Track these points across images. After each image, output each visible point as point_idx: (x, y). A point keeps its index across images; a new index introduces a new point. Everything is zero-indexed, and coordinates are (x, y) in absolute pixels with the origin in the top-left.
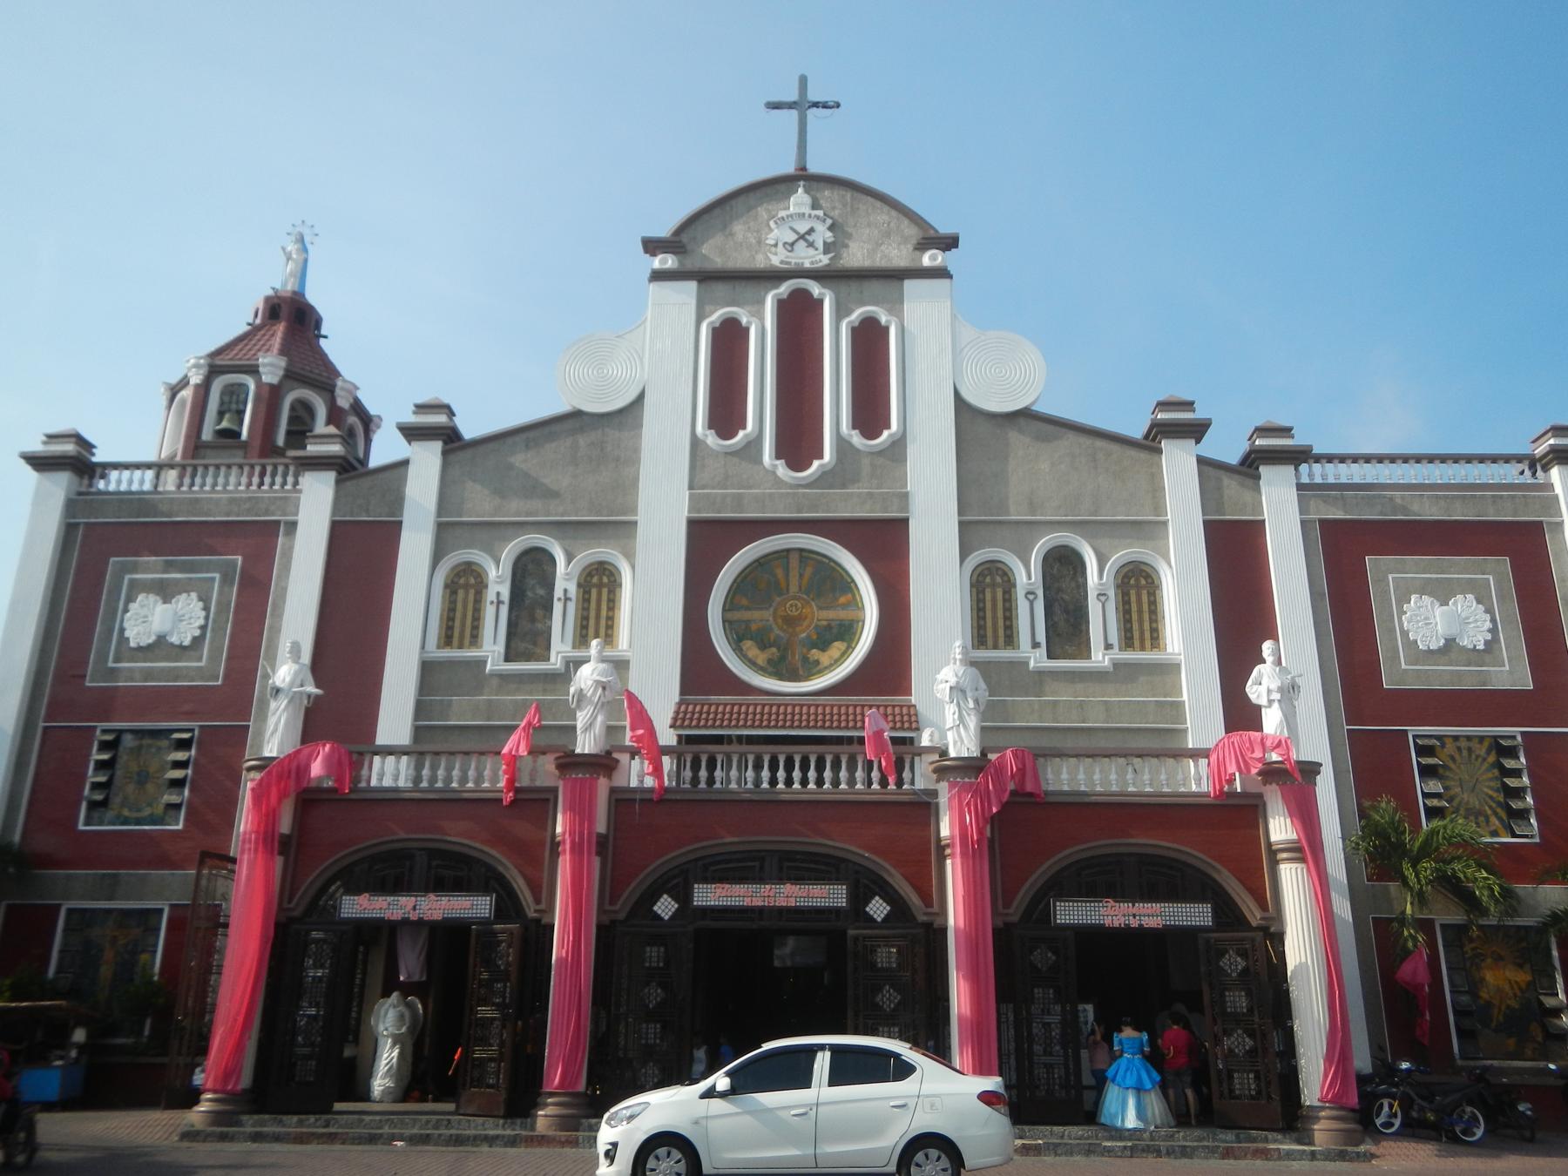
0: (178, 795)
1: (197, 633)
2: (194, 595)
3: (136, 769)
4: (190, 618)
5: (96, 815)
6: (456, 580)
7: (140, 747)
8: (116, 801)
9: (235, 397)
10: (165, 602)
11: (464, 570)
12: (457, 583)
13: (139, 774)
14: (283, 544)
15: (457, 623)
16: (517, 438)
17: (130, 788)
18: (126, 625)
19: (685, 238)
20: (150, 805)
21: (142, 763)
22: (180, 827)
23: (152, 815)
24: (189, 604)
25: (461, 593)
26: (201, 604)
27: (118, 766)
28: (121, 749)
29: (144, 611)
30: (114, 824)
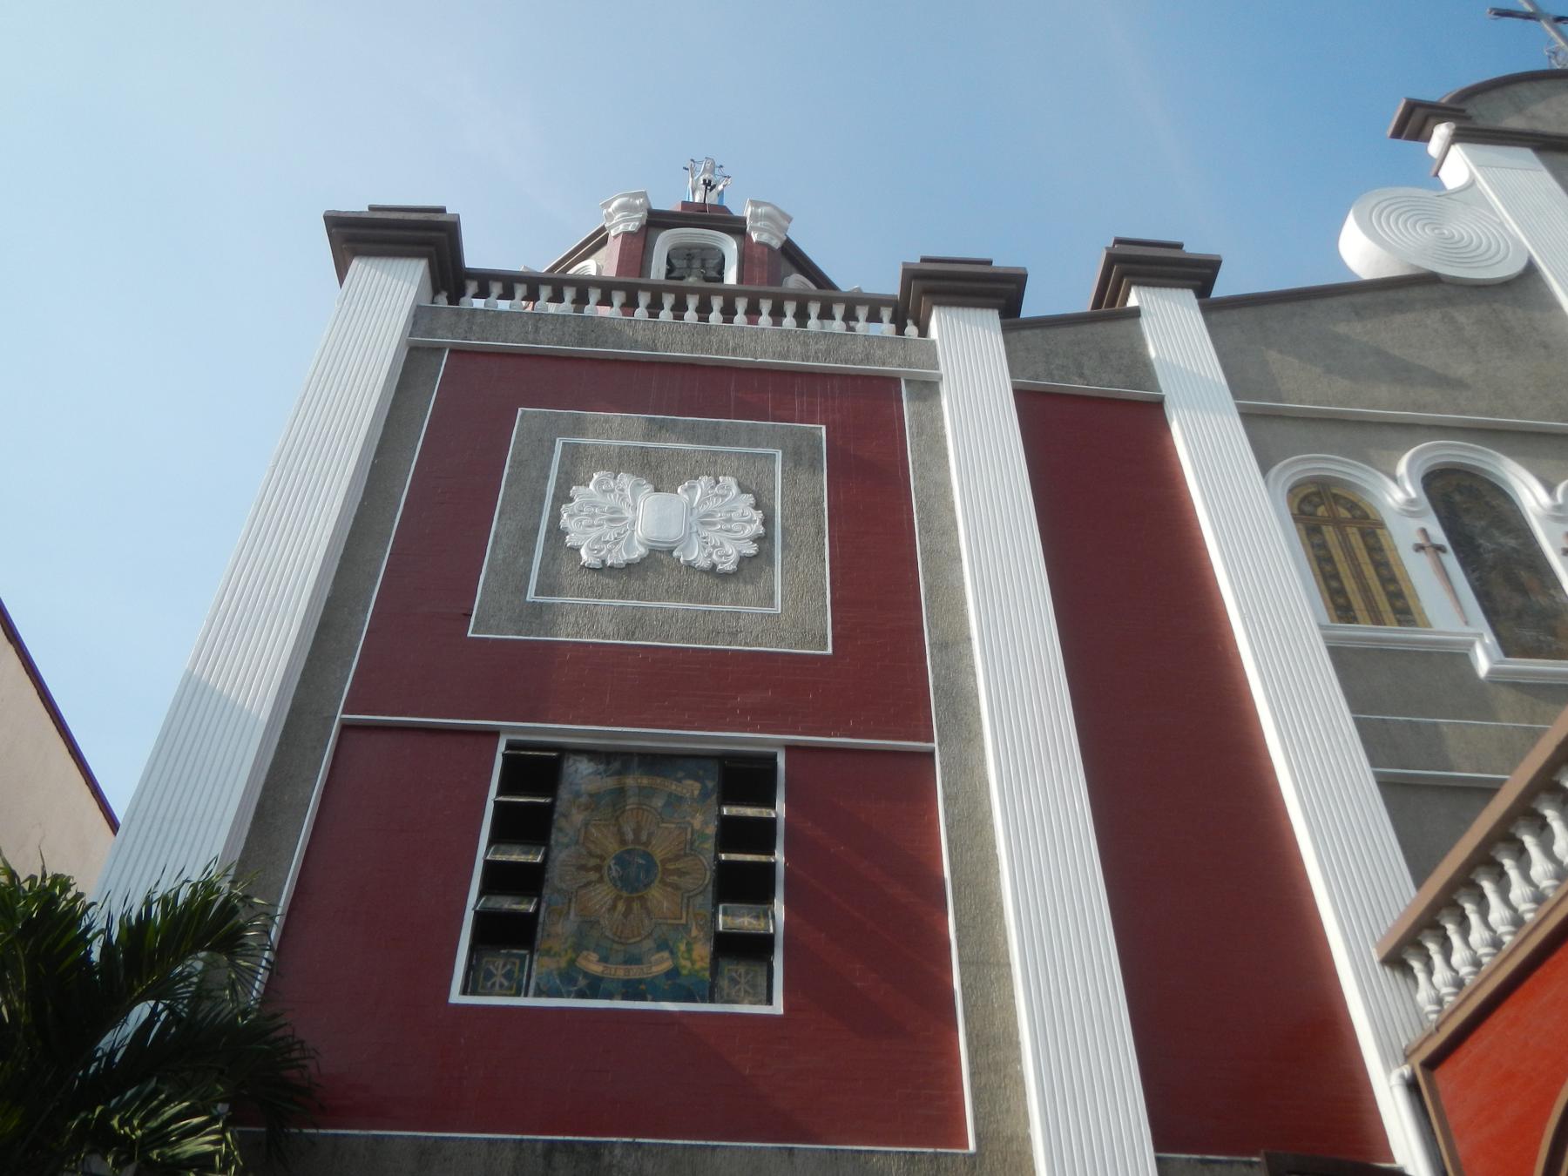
0: (757, 917)
1: (751, 549)
2: (729, 482)
3: (613, 847)
4: (729, 520)
5: (498, 964)
6: (1307, 508)
7: (621, 792)
8: (558, 930)
9: (696, 264)
10: (657, 490)
11: (1318, 494)
12: (1313, 514)
13: (620, 860)
14: (913, 415)
15: (1350, 585)
16: (1334, 302)
17: (601, 896)
18: (565, 521)
19: (1471, 108)
20: (663, 945)
21: (630, 836)
22: (778, 1007)
23: (674, 973)
24: (726, 496)
25: (1330, 534)
26: (749, 498)
27: (555, 836)
28: (564, 793)
29: (612, 500)
30: (557, 994)
